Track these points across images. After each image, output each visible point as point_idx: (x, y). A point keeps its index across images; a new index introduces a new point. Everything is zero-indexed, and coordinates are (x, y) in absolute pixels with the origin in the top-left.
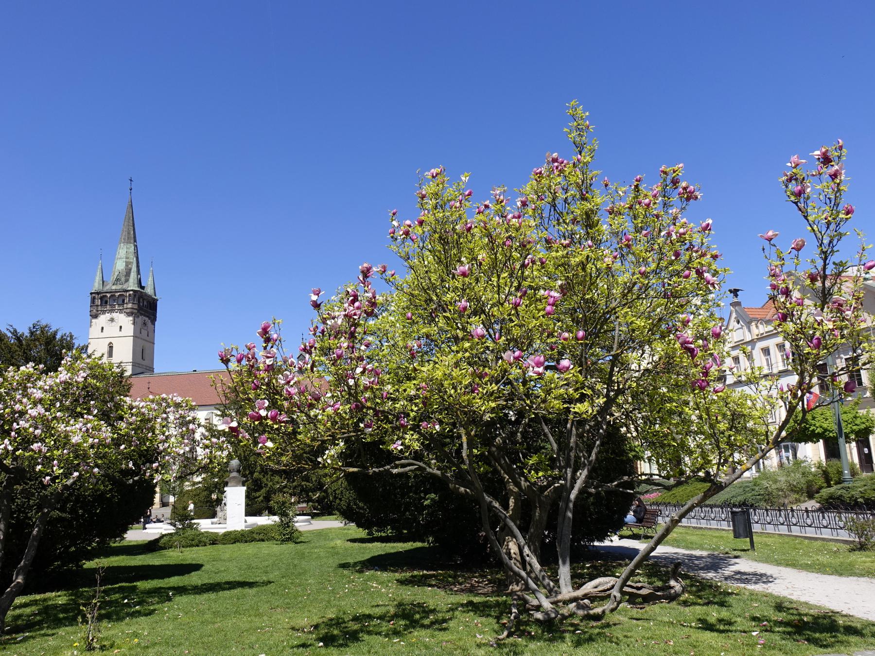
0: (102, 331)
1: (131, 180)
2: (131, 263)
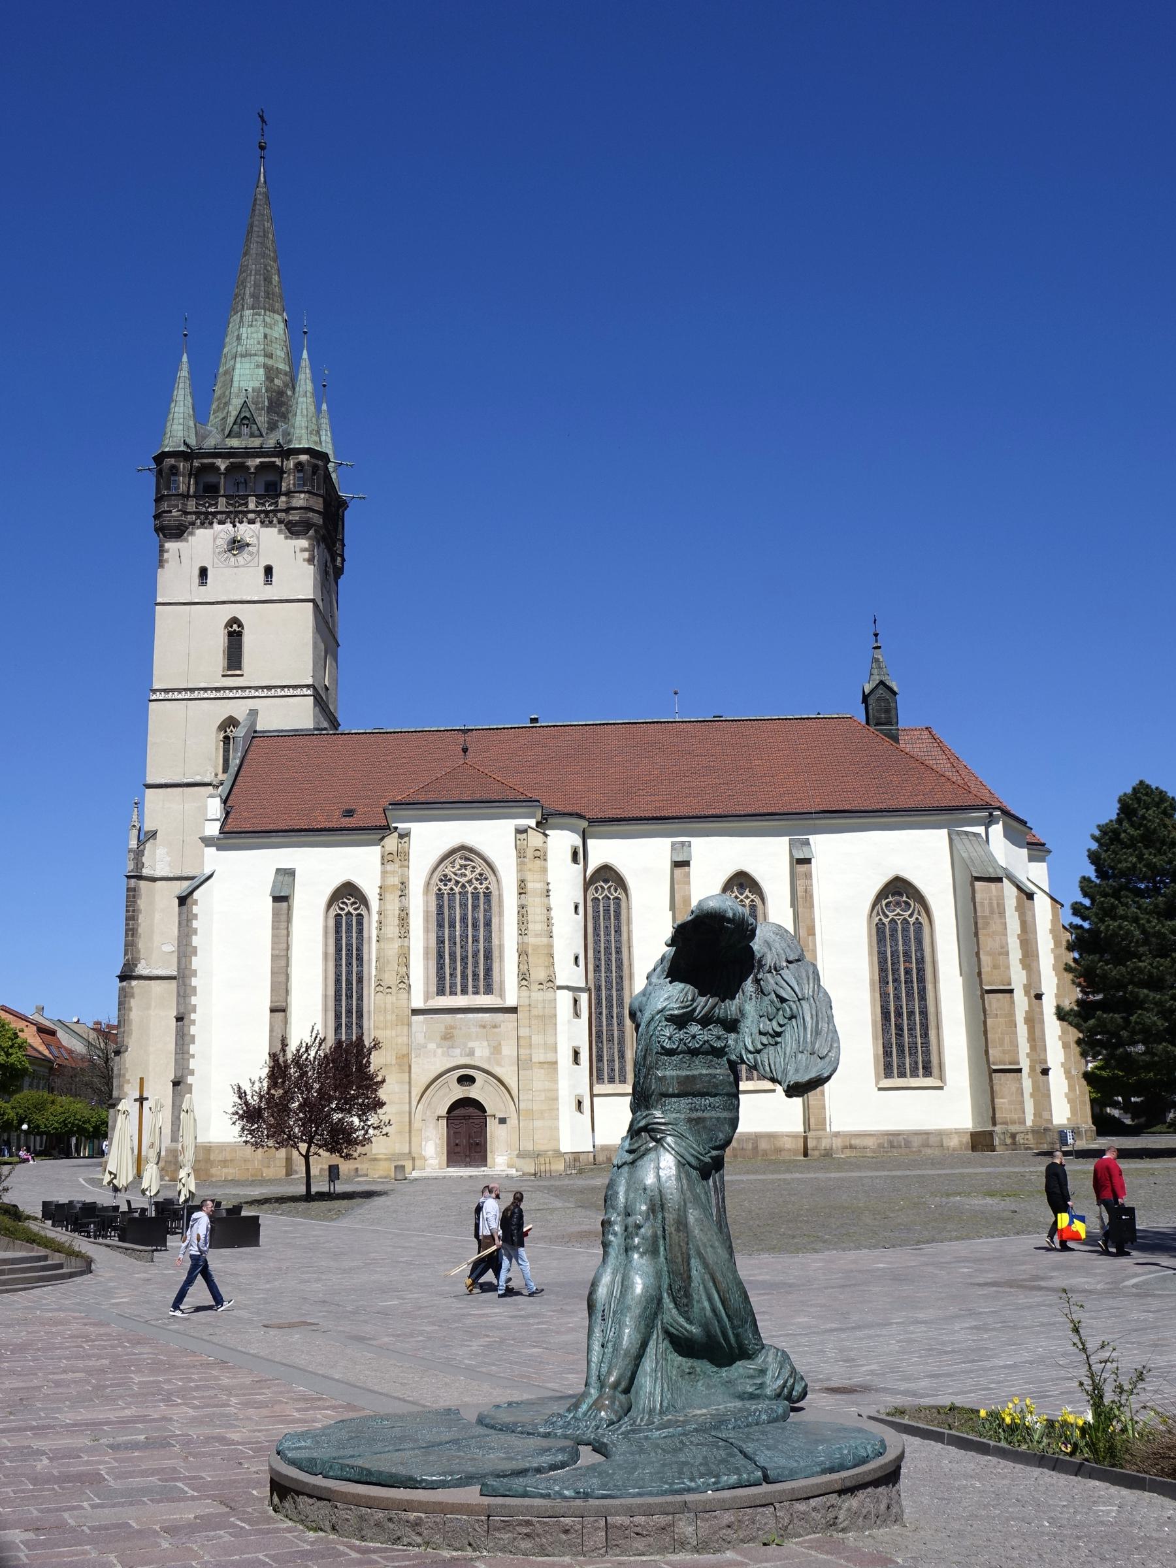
1: (262, 117)
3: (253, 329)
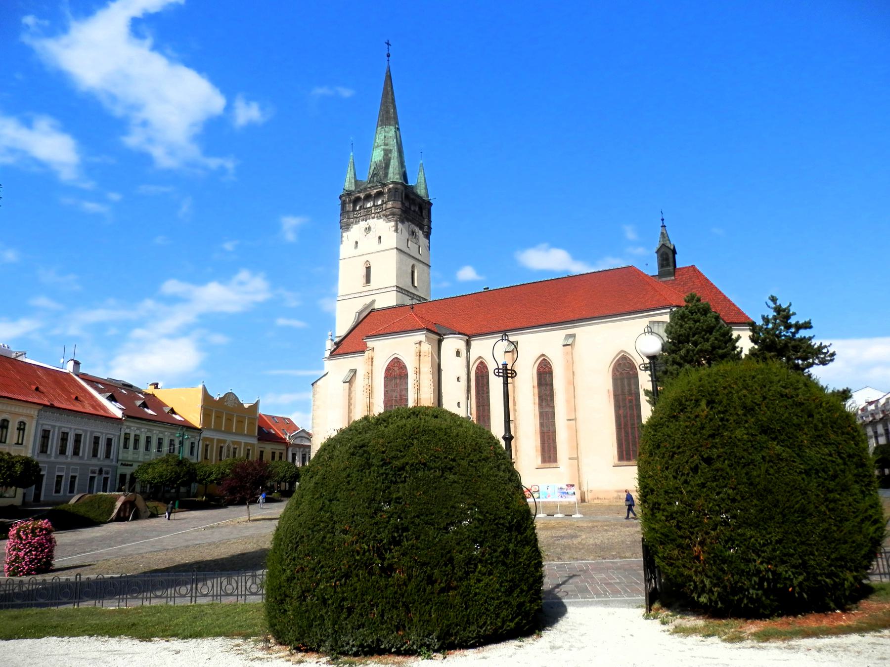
2: (391, 151)
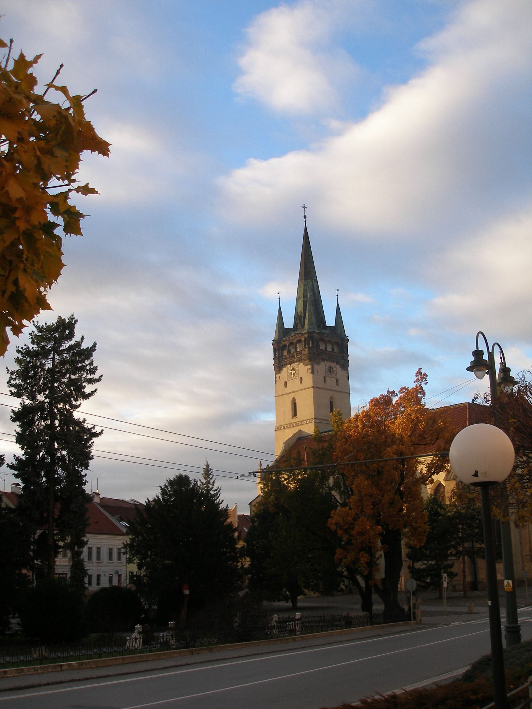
0: (286, 387)
1: (304, 207)
3: (301, 289)
